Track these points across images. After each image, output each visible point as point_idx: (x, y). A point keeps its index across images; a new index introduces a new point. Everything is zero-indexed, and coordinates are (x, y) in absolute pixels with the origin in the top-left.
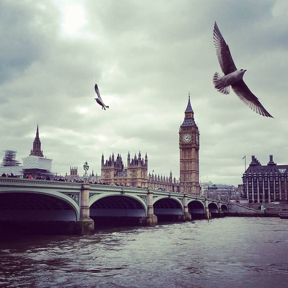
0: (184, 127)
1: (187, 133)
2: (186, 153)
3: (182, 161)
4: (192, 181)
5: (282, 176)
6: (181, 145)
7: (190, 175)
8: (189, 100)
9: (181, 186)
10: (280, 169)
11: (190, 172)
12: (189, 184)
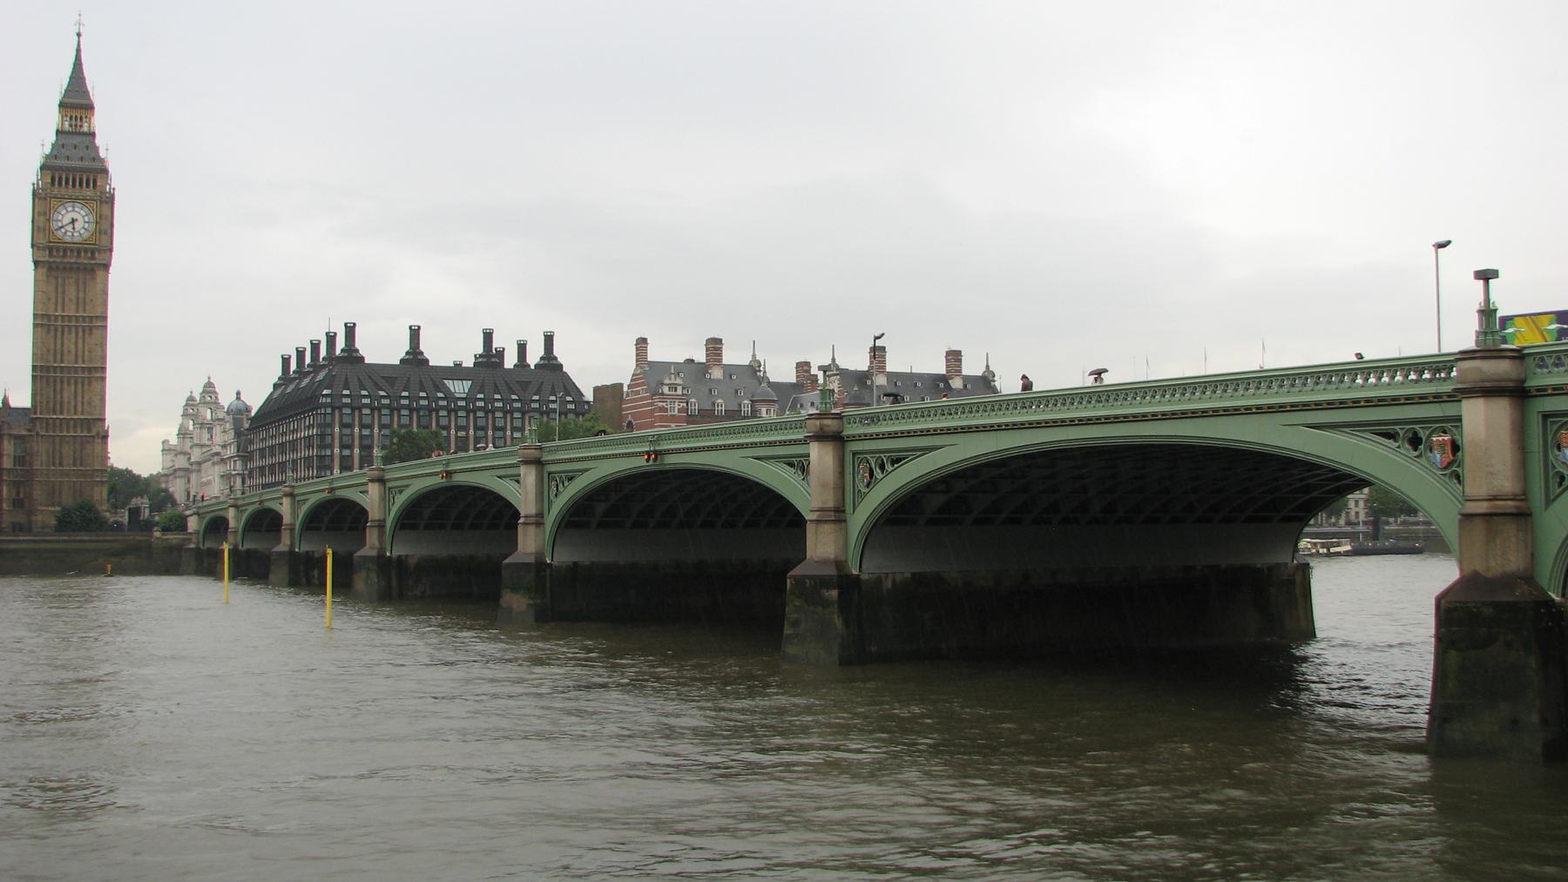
0: (61, 169)
1: (75, 199)
2: (64, 285)
3: (43, 322)
4: (89, 414)
5: (461, 408)
6: (44, 249)
7: (80, 386)
8: (78, 51)
9: (38, 434)
10: (451, 381)
11: (80, 373)
12: (75, 427)
